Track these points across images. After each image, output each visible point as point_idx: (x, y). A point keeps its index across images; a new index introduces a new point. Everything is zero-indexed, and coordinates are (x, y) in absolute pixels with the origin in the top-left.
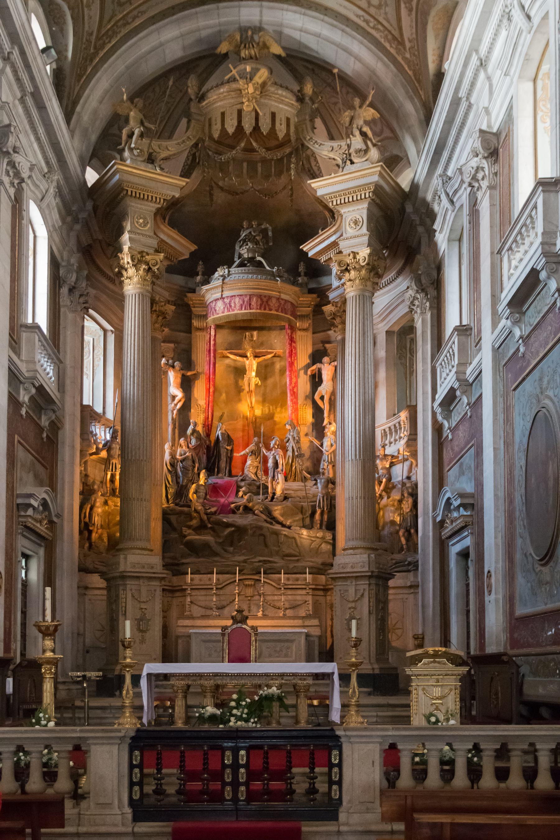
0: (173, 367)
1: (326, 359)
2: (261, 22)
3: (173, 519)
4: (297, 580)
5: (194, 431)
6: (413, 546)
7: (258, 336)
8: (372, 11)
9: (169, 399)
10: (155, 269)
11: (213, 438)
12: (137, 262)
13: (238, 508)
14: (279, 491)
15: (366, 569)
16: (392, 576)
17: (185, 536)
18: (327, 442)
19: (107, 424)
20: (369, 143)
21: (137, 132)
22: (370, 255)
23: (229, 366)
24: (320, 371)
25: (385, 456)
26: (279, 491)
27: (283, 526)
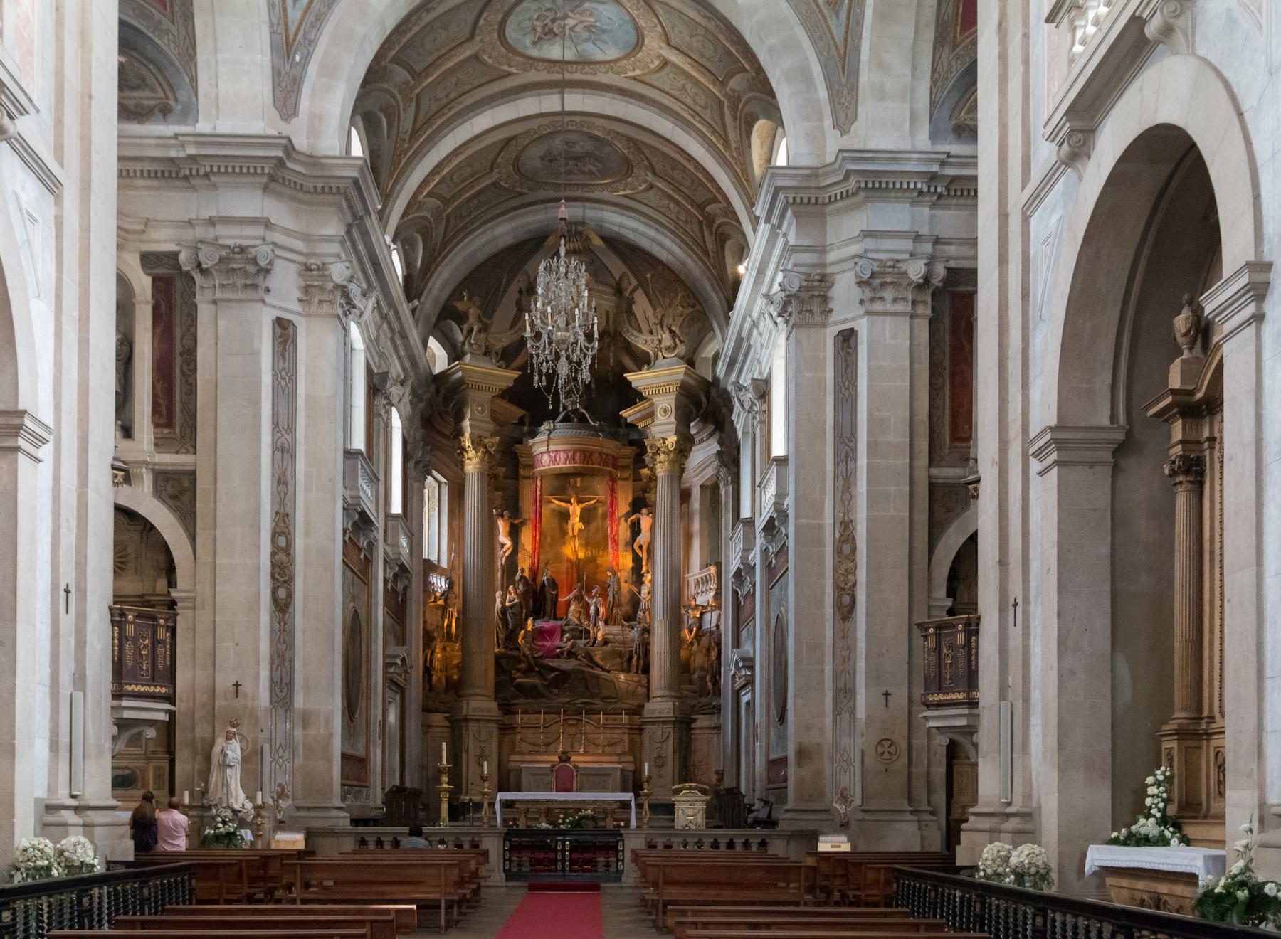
0: (502, 516)
1: (644, 511)
2: (584, 217)
3: (504, 662)
4: (615, 720)
5: (522, 577)
6: (717, 691)
7: (582, 482)
8: (680, 223)
9: (499, 546)
10: (492, 450)
11: (539, 581)
12: (477, 443)
13: (562, 653)
14: (600, 634)
15: (671, 715)
16: (695, 720)
17: (515, 679)
18: (645, 590)
19: (442, 572)
20: (677, 341)
21: (475, 329)
22: (677, 442)
23: (554, 511)
24: (639, 521)
25: (697, 606)
26: (599, 638)
27: (603, 669)
